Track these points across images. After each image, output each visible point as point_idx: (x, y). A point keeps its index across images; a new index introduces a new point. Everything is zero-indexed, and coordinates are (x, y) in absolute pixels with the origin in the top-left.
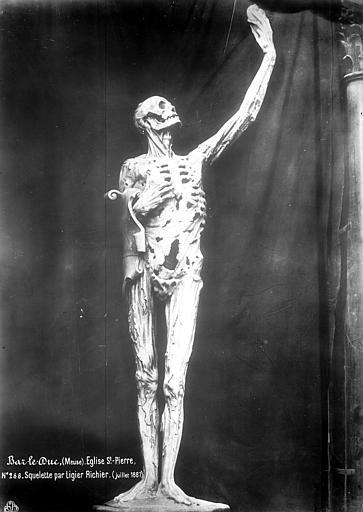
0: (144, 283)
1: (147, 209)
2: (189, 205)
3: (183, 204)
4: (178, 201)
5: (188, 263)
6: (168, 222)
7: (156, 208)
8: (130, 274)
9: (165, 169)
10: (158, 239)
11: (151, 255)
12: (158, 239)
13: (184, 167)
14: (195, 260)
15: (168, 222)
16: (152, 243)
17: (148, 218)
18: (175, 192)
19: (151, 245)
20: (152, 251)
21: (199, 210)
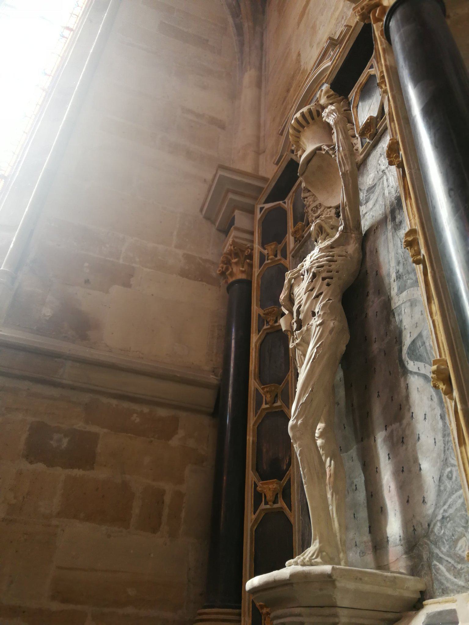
4: (304, 276)
5: (314, 314)
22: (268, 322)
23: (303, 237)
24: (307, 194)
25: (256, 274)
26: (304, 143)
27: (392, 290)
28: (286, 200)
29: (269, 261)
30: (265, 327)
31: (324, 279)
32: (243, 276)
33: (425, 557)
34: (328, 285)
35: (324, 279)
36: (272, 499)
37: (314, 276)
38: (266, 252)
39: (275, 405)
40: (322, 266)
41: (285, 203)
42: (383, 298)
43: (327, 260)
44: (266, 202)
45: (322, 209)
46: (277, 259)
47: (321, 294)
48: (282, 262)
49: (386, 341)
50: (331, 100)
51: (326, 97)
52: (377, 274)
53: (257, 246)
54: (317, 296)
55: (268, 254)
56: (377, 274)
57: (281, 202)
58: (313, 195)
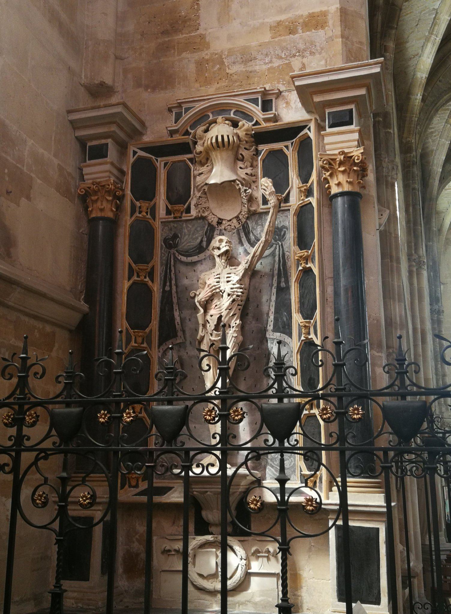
0: (205, 341)
1: (203, 300)
2: (229, 295)
3: (225, 295)
4: (223, 293)
5: (230, 326)
6: (216, 306)
7: (209, 299)
8: (198, 338)
9: (218, 276)
10: (211, 316)
11: (208, 325)
12: (211, 316)
13: (230, 274)
14: (234, 325)
15: (216, 306)
16: (208, 318)
17: (206, 305)
18: (221, 289)
19: (208, 319)
20: (209, 323)
21: (234, 297)
22: (138, 276)
23: (180, 217)
24: (204, 196)
25: (129, 223)
26: (216, 156)
27: (268, 326)
28: (159, 159)
29: (141, 215)
30: (136, 278)
31: (238, 305)
32: (110, 215)
33: (263, 464)
34: (239, 310)
35: (238, 305)
36: (139, 410)
37: (234, 301)
38: (138, 204)
39: (142, 345)
40: (238, 296)
41: (157, 160)
42: (260, 325)
43: (241, 292)
44: (141, 149)
45: (208, 212)
46: (147, 216)
47: (235, 314)
48: (150, 221)
49: (257, 352)
50: (247, 137)
51: (245, 133)
52: (257, 307)
53: (128, 192)
54: (234, 315)
55: (140, 207)
56: (257, 307)
57: (153, 157)
58: (207, 198)
